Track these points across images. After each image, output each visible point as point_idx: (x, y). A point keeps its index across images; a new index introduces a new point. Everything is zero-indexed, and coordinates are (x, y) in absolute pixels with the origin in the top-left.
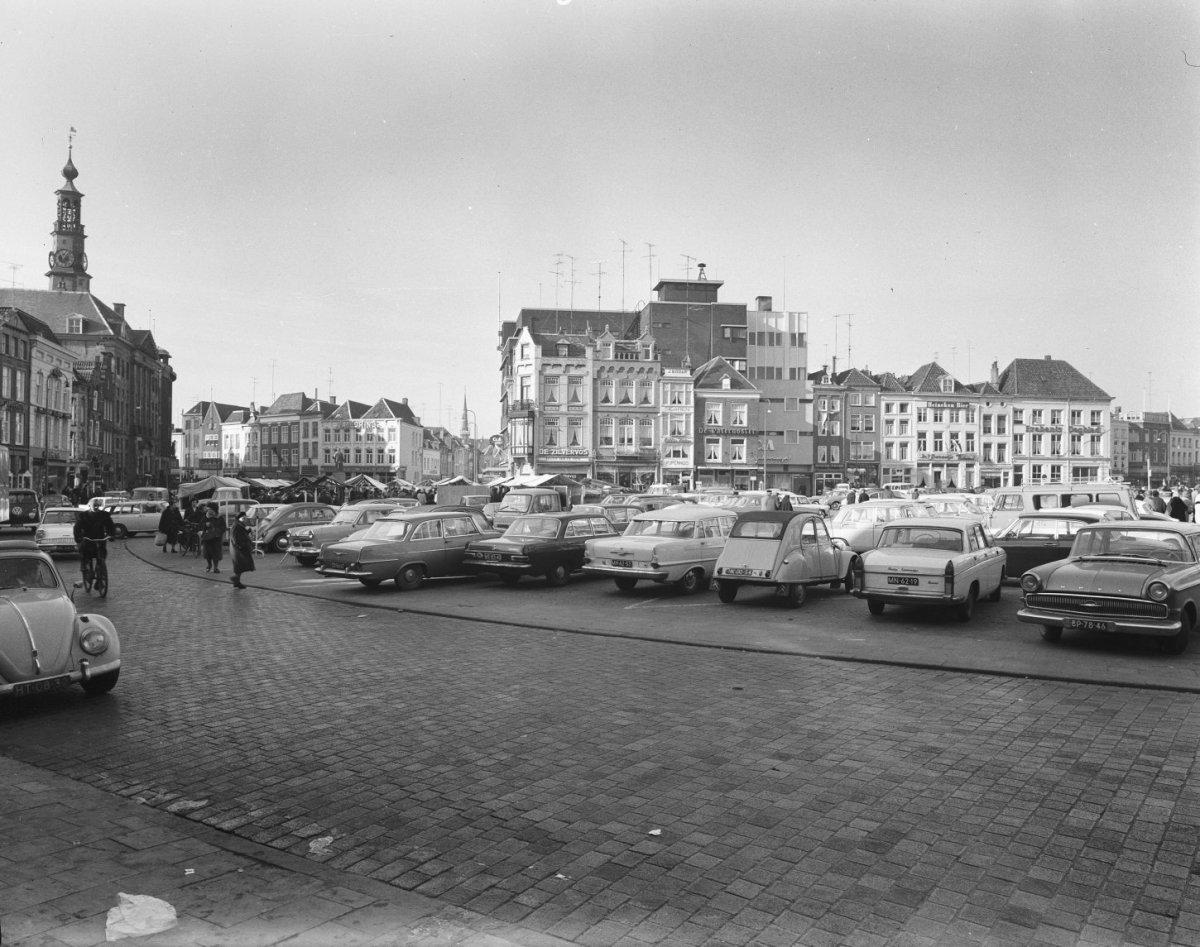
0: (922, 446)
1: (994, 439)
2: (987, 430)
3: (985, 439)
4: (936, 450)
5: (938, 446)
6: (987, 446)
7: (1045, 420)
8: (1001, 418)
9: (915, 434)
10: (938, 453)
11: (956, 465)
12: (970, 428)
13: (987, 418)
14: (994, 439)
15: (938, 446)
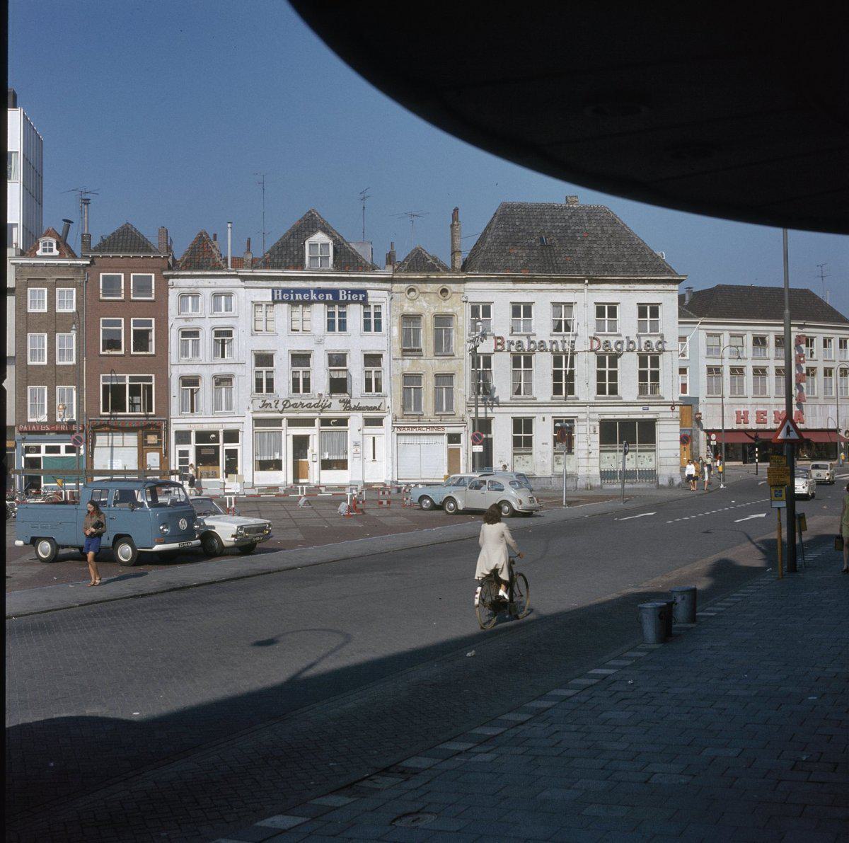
0: (264, 385)
1: (429, 365)
2: (410, 348)
3: (408, 365)
4: (296, 389)
5: (301, 385)
6: (411, 380)
7: (542, 324)
8: (443, 321)
9: (250, 361)
10: (301, 397)
11: (343, 422)
12: (374, 343)
13: (410, 321)
14: (429, 365)
15: (301, 385)
